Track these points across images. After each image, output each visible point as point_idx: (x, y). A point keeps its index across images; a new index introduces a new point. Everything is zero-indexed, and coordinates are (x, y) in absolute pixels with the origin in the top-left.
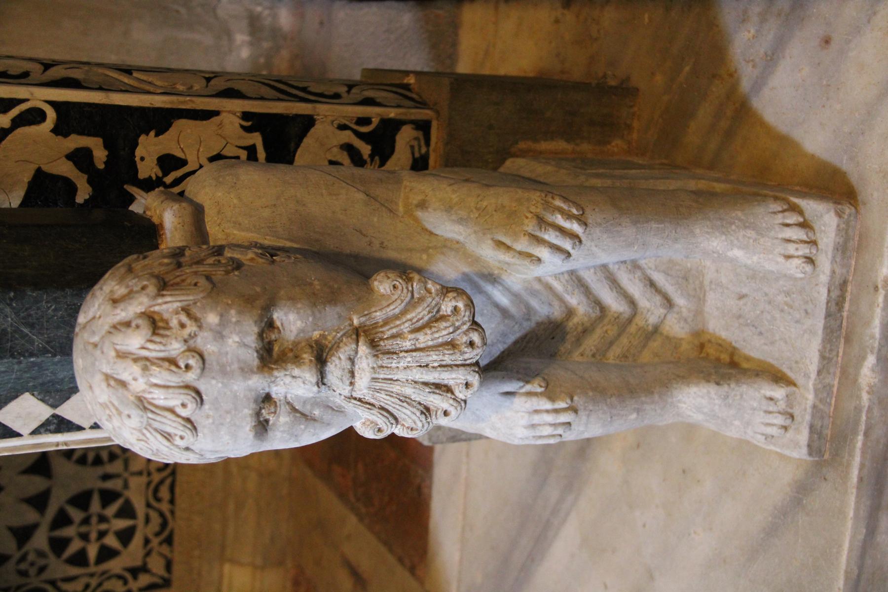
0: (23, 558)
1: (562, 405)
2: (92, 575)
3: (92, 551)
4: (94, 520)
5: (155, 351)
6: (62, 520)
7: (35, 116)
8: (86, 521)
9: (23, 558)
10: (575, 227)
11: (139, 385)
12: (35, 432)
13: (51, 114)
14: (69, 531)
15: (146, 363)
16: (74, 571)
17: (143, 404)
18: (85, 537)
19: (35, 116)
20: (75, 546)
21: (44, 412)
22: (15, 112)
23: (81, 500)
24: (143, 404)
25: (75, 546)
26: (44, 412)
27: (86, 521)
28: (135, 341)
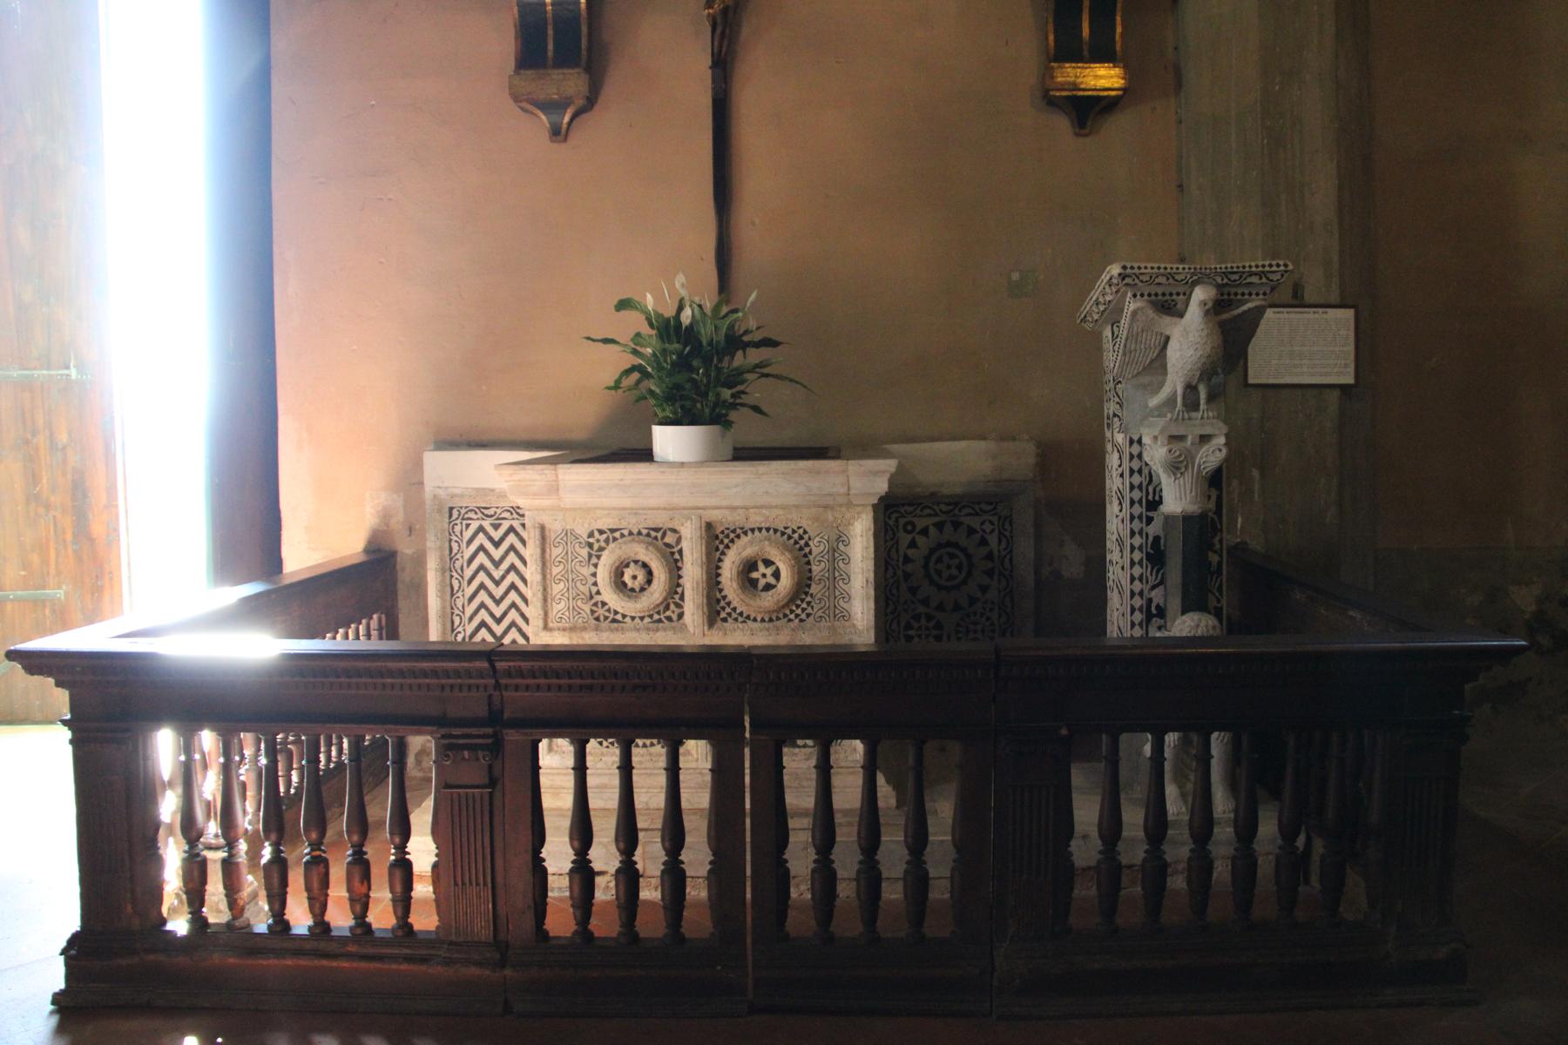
0: (913, 602)
1: (1176, 743)
2: (899, 633)
3: (911, 633)
4: (927, 632)
5: (1210, 628)
6: (929, 618)
7: (1219, 601)
8: (927, 629)
9: (913, 602)
10: (1225, 740)
11: (1202, 625)
12: (1131, 605)
13: (1219, 605)
14: (923, 621)
15: (1207, 626)
16: (903, 624)
17: (1198, 626)
18: (920, 628)
19: (1219, 601)
20: (916, 625)
21: (1137, 606)
22: (1220, 597)
23: (939, 626)
24: (1198, 626)
25: (916, 625)
26: (1137, 606)
27: (927, 629)
28: (1210, 623)
